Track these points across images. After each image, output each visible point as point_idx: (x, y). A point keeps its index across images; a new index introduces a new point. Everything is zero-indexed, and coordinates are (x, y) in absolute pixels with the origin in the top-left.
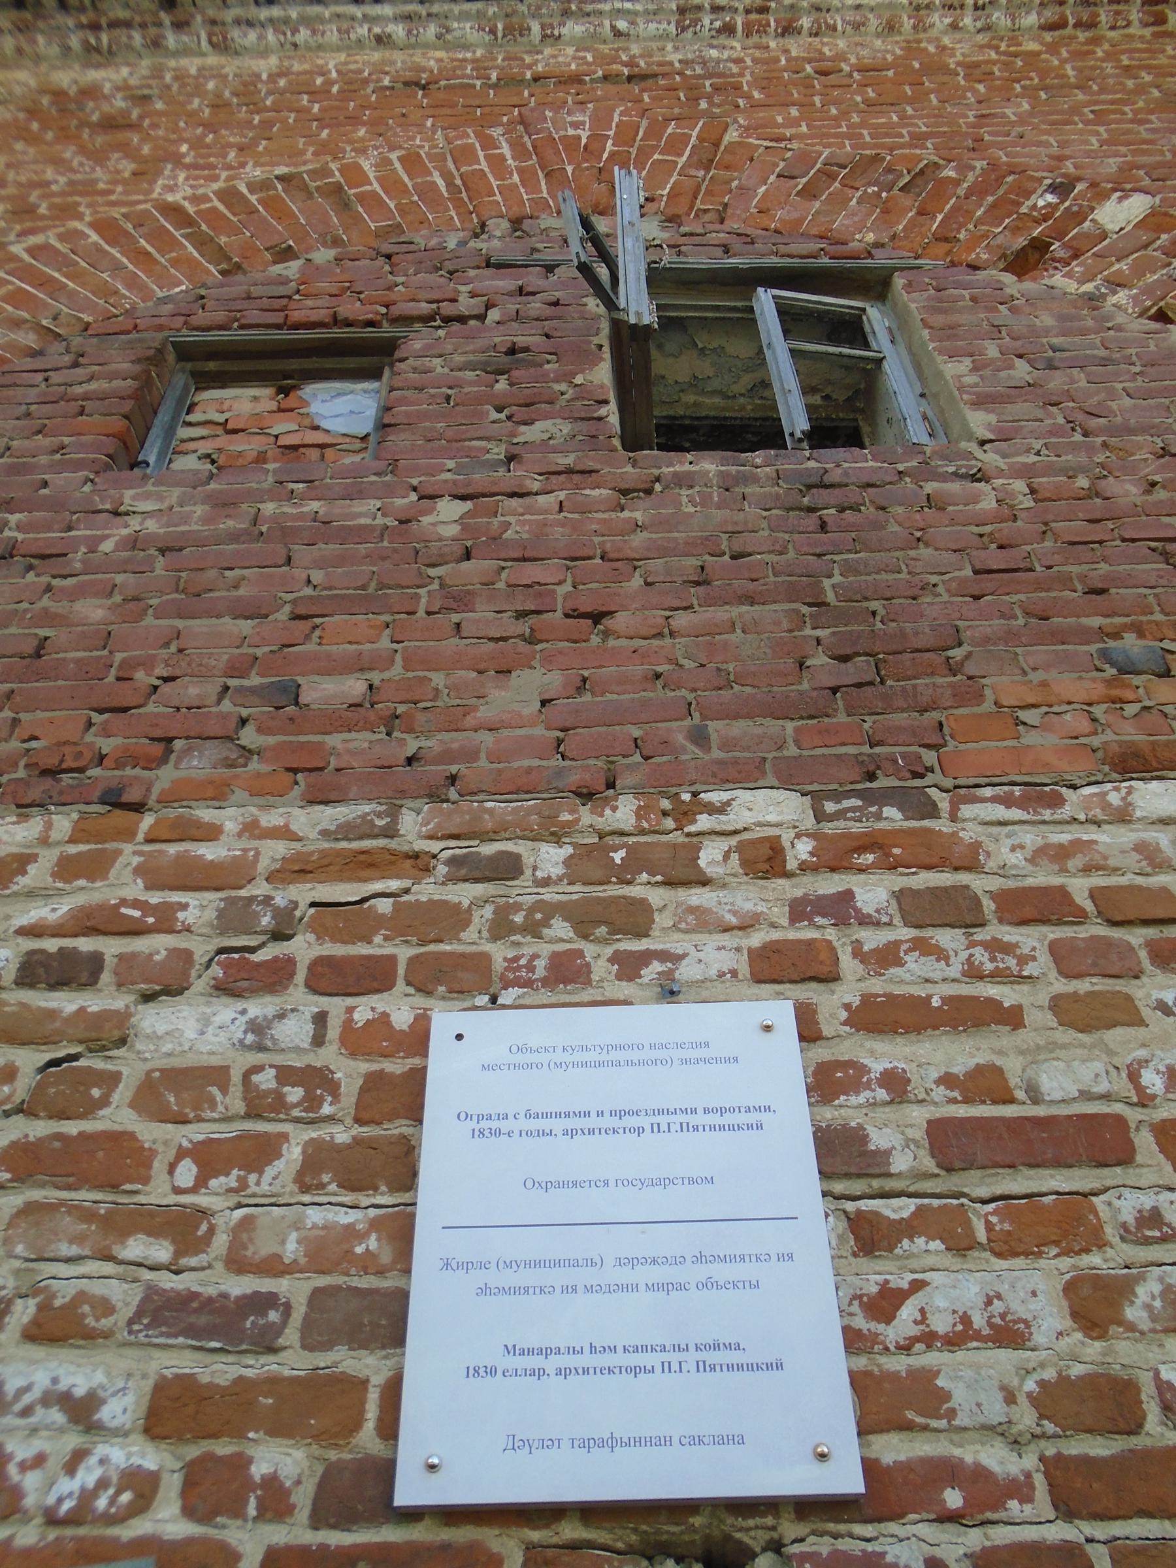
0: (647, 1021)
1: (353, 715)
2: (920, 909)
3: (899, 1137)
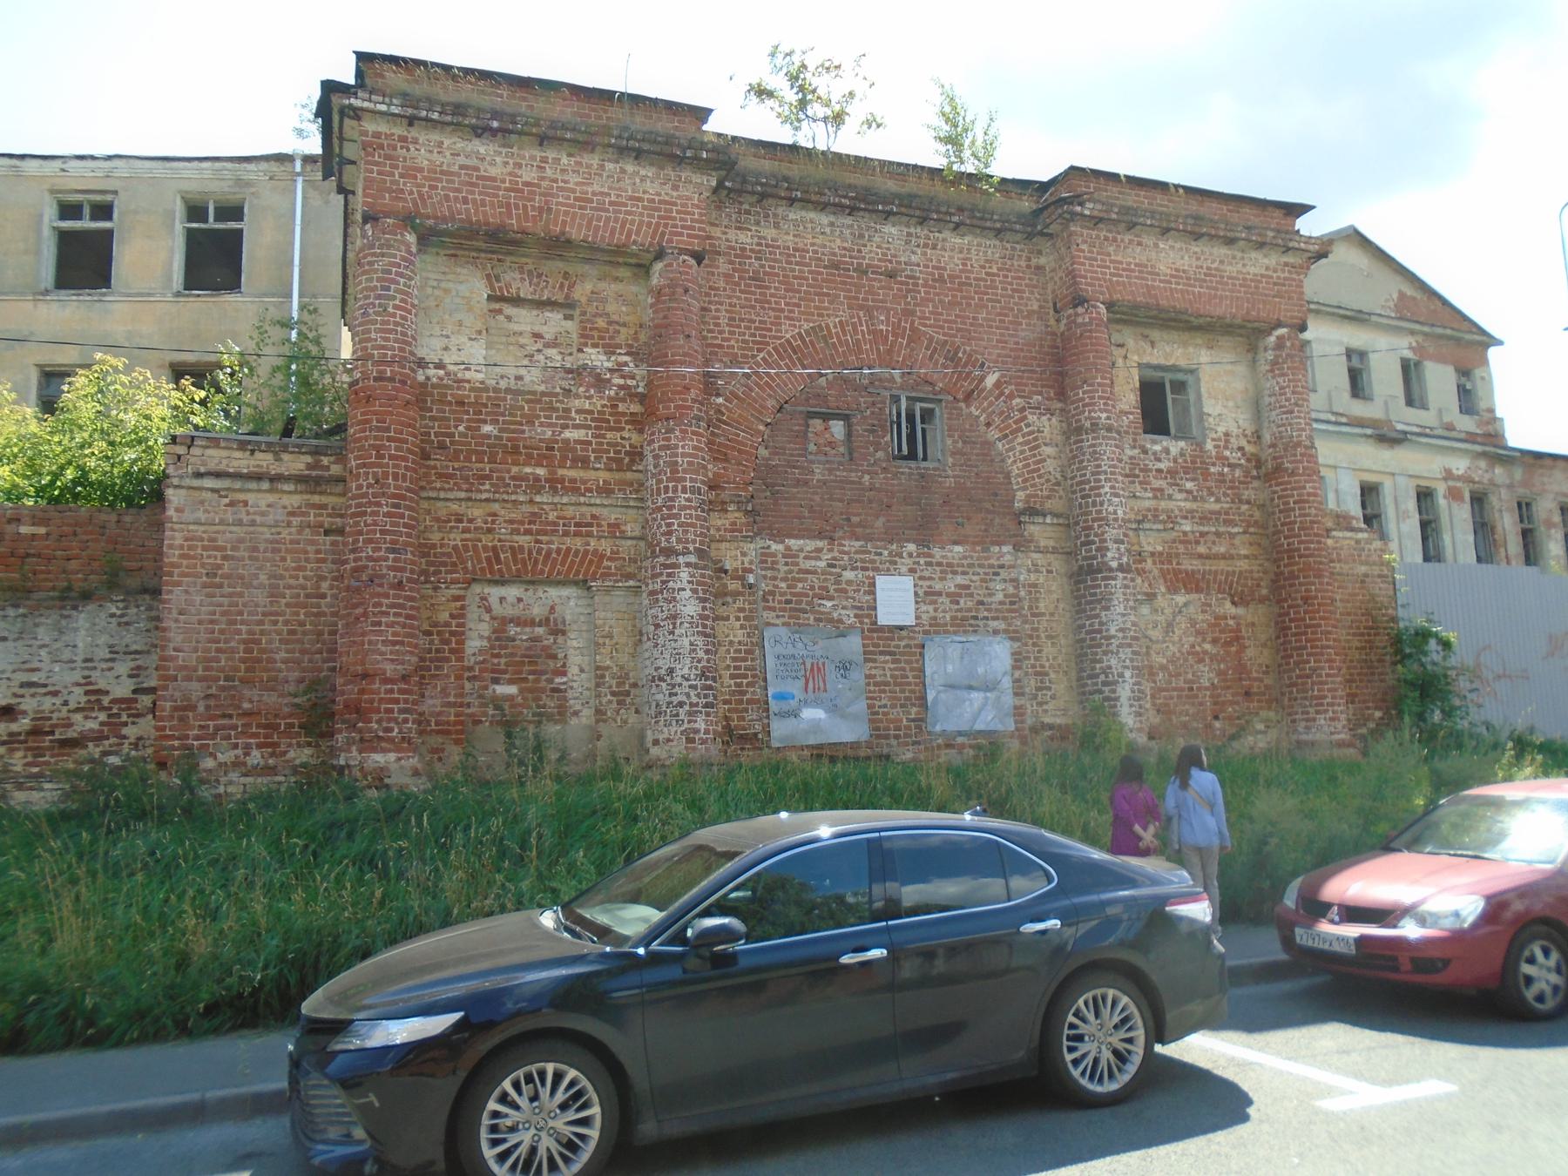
0: (898, 578)
1: (859, 525)
2: (929, 564)
3: (921, 592)
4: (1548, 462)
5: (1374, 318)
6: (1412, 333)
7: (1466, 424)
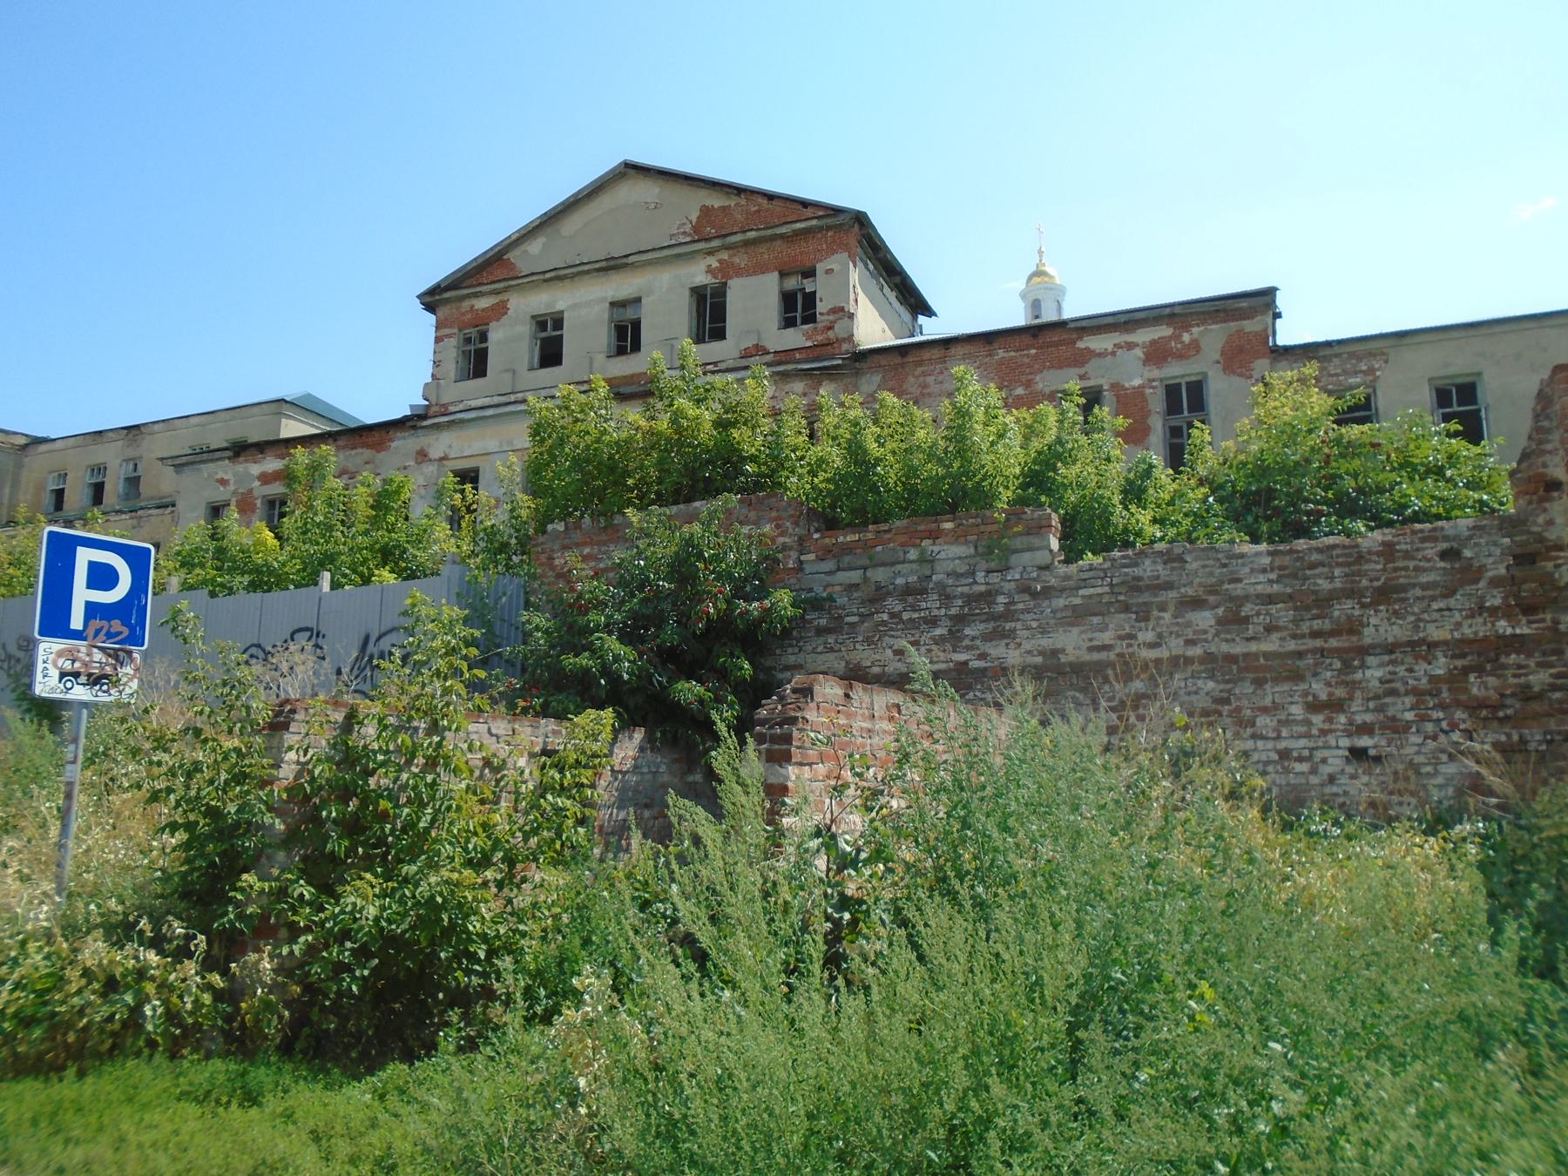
4: (936, 353)
5: (631, 259)
6: (710, 253)
7: (795, 338)
